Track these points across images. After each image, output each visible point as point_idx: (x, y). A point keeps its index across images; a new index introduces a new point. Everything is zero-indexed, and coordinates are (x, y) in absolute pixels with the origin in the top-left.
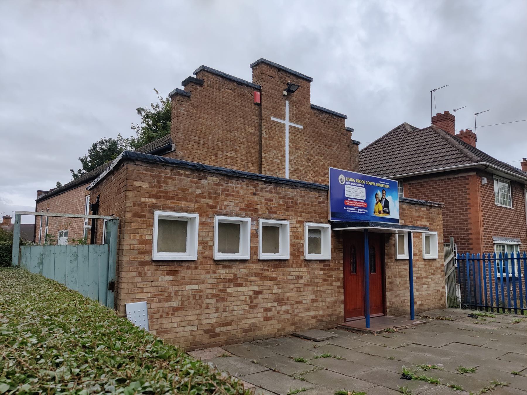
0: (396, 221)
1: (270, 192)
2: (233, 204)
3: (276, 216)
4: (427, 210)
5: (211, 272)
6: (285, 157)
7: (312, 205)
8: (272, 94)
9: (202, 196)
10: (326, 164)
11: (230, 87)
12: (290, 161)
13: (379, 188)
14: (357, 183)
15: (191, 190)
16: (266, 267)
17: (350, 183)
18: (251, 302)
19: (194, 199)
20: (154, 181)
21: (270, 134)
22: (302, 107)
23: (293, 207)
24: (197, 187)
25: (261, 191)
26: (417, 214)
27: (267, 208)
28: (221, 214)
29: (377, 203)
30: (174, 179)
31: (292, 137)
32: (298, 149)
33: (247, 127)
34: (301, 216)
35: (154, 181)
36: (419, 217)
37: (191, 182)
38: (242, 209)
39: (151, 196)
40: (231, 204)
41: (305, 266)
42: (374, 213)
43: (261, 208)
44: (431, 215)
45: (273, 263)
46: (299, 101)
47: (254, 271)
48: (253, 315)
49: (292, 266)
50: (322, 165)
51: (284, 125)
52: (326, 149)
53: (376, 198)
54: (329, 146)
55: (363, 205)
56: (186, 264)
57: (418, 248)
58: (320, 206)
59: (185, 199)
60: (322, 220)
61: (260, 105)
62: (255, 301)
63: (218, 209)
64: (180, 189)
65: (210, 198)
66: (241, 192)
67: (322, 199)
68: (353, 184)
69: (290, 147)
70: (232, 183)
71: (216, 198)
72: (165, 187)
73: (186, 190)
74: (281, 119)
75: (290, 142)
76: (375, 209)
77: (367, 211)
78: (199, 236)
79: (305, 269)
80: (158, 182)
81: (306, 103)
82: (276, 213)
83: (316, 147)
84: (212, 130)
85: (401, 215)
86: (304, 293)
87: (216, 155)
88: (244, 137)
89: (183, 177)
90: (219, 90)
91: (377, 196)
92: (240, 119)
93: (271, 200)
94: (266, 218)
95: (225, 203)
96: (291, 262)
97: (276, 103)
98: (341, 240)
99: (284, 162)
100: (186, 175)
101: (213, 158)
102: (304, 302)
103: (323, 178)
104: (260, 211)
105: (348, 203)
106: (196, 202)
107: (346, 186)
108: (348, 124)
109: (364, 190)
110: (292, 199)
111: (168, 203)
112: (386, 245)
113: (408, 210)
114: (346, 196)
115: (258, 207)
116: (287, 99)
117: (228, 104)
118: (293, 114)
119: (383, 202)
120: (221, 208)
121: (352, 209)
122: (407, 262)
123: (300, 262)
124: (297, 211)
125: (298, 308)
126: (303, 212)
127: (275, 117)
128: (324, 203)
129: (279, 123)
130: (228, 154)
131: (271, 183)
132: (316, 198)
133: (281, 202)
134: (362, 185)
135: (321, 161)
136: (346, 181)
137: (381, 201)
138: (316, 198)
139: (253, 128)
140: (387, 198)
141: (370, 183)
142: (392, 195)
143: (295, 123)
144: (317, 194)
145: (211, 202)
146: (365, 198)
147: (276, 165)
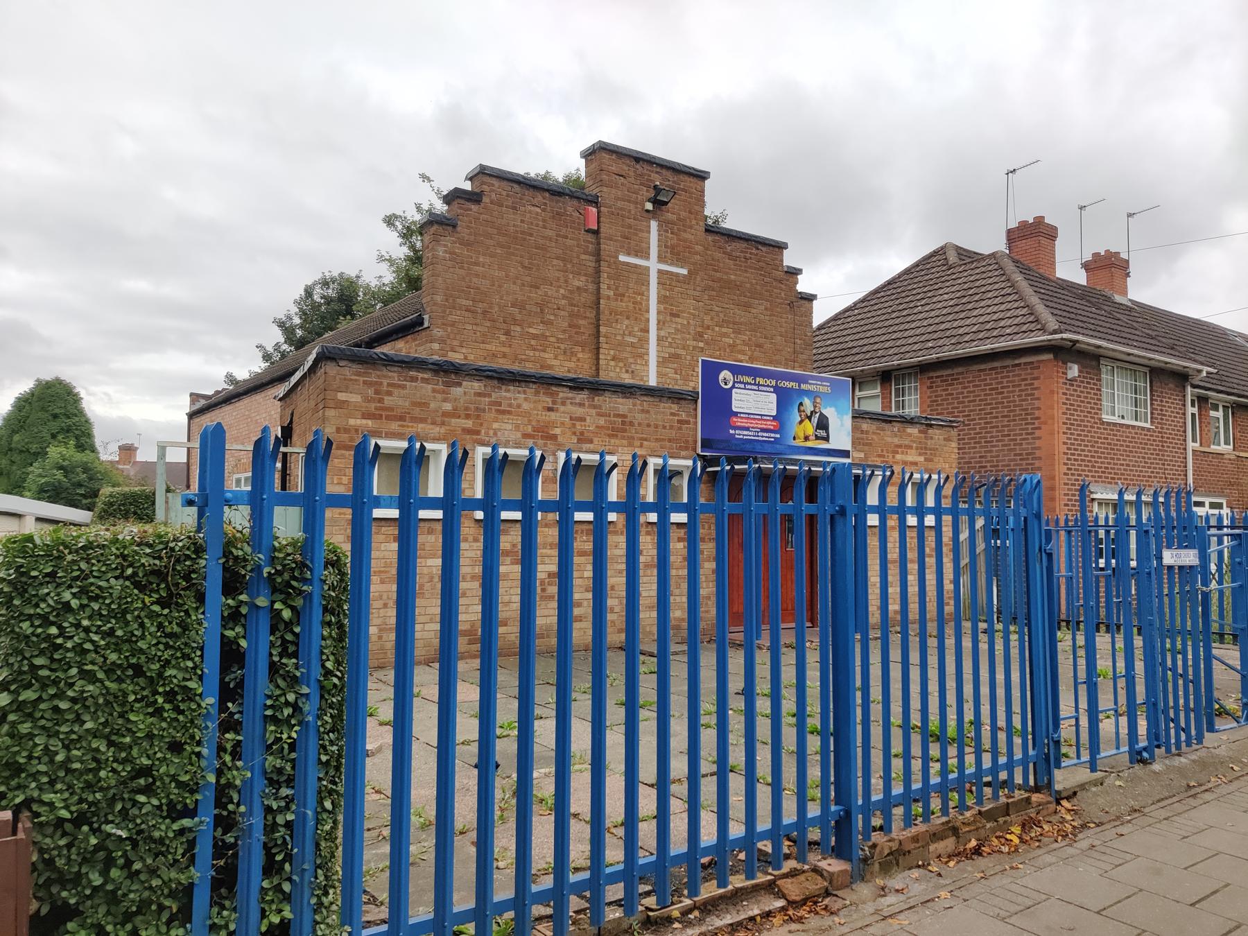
0: (845, 454)
1: (581, 405)
2: (509, 427)
3: (591, 446)
4: (920, 432)
5: (471, 538)
6: (648, 331)
7: (664, 427)
8: (621, 209)
9: (454, 414)
11: (535, 202)
12: (659, 339)
14: (759, 385)
15: (432, 405)
19: (439, 420)
20: (370, 392)
21: (617, 289)
23: (625, 431)
24: (445, 400)
25: (563, 404)
26: (896, 441)
27: (574, 433)
30: (404, 387)
31: (663, 292)
32: (678, 316)
34: (641, 446)
35: (370, 392)
36: (900, 446)
37: (434, 391)
39: (366, 416)
43: (563, 433)
44: (929, 442)
46: (679, 219)
50: (730, 346)
51: (648, 269)
54: (747, 306)
55: (771, 425)
56: (427, 525)
58: (680, 429)
59: (423, 420)
60: (683, 453)
61: (596, 233)
63: (483, 436)
64: (414, 404)
65: (468, 417)
66: (525, 406)
67: (684, 416)
69: (659, 313)
70: (509, 391)
71: (478, 417)
72: (388, 401)
73: (424, 405)
74: (641, 257)
75: (659, 302)
80: (377, 392)
81: (694, 222)
82: (591, 442)
84: (500, 286)
85: (854, 443)
87: (507, 333)
88: (564, 297)
89: (419, 384)
90: (514, 208)
92: (555, 262)
93: (582, 419)
95: (495, 425)
97: (630, 227)
99: (647, 341)
100: (425, 380)
101: (503, 338)
104: (560, 439)
105: (738, 422)
106: (443, 424)
109: (774, 397)
110: (624, 416)
115: (557, 431)
116: (654, 218)
117: (531, 235)
118: (666, 247)
119: (815, 419)
120: (487, 434)
124: (633, 438)
127: (629, 254)
128: (688, 422)
129: (636, 266)
130: (531, 330)
131: (582, 389)
132: (672, 414)
133: (602, 422)
137: (809, 418)
138: (672, 414)
139: (583, 278)
142: (836, 407)
143: (671, 264)
144: (675, 407)
145: (469, 424)
146: (774, 413)
147: (629, 349)
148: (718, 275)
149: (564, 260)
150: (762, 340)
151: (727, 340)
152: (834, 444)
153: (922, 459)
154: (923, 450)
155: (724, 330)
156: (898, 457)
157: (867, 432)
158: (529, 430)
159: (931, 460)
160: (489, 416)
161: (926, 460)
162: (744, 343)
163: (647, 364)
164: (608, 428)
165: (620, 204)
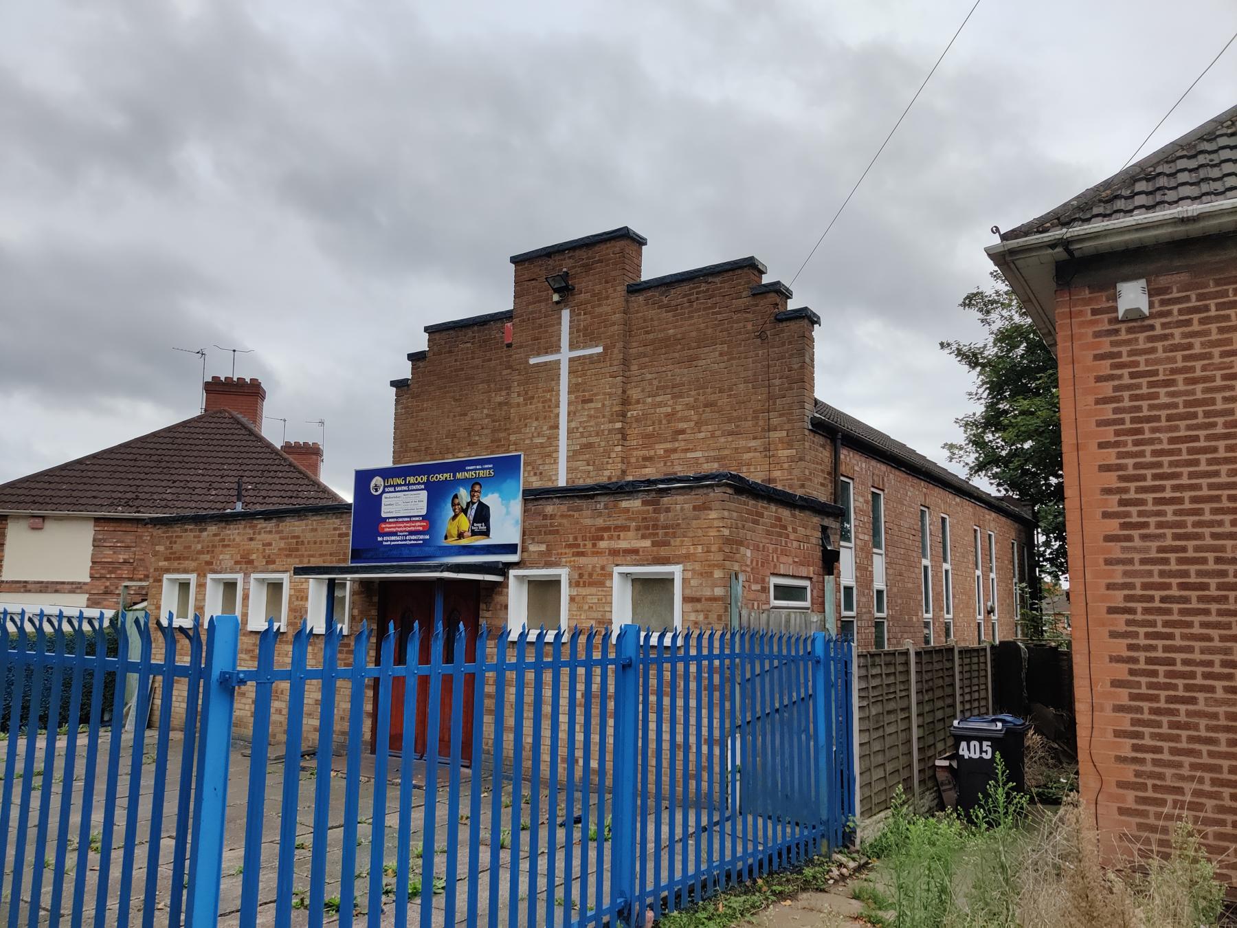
0: (511, 549)
1: (270, 532)
4: (644, 503)
6: (557, 427)
8: (532, 313)
10: (679, 408)
11: (466, 339)
12: (570, 431)
13: (462, 482)
14: (409, 484)
17: (392, 489)
22: (600, 305)
23: (297, 550)
26: (600, 522)
28: (215, 572)
31: (574, 381)
32: (591, 401)
36: (607, 529)
39: (167, 559)
40: (226, 558)
42: (446, 538)
44: (662, 517)
46: (594, 295)
50: (668, 415)
51: (571, 360)
53: (453, 505)
55: (419, 526)
58: (340, 542)
59: (186, 559)
63: (214, 566)
64: (185, 547)
69: (569, 404)
74: (552, 353)
75: (569, 393)
82: (274, 562)
83: (649, 376)
90: (450, 352)
91: (457, 501)
92: (480, 386)
93: (270, 544)
98: (376, 599)
99: (556, 438)
103: (669, 446)
105: (386, 528)
108: (405, 371)
110: (298, 537)
111: (175, 564)
112: (483, 606)
113: (562, 516)
114: (383, 515)
115: (254, 556)
116: (566, 307)
117: (462, 369)
119: (472, 512)
121: (393, 538)
124: (303, 556)
126: (312, 556)
127: (538, 355)
129: (546, 363)
132: (335, 529)
133: (282, 545)
135: (666, 405)
137: (465, 511)
138: (335, 529)
140: (484, 500)
142: (500, 492)
143: (583, 348)
144: (338, 521)
146: (424, 512)
147: (537, 451)
148: (651, 336)
149: (488, 382)
150: (713, 397)
151: (663, 410)
152: (495, 538)
153: (647, 543)
154: (647, 528)
155: (658, 399)
156: (603, 544)
157: (552, 517)
159: (666, 544)
160: (217, 550)
161: (654, 544)
162: (689, 407)
163: (556, 462)
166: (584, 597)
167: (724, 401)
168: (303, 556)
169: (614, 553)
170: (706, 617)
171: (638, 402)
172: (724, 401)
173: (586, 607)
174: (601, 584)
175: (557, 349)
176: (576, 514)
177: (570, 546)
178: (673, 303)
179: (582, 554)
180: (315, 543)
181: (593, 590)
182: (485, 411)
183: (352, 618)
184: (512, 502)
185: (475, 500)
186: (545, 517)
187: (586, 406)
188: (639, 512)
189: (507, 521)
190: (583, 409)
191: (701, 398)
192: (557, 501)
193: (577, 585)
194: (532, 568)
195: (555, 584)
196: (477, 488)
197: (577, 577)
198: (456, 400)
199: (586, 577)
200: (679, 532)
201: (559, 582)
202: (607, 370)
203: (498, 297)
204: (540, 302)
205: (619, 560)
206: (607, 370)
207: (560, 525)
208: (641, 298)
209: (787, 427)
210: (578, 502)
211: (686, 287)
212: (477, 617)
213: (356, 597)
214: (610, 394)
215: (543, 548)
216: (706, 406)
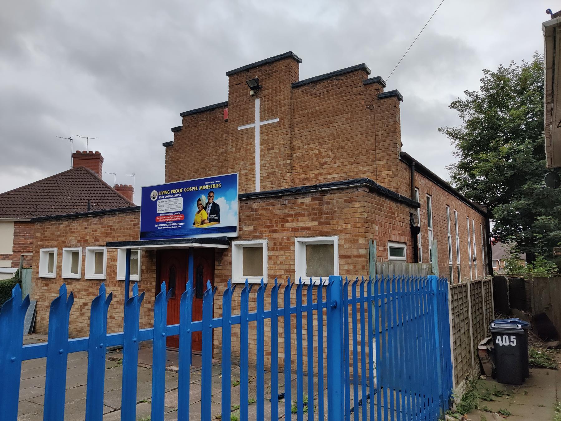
0: (232, 229)
1: (96, 224)
2: (74, 238)
4: (313, 199)
6: (254, 164)
8: (239, 102)
10: (323, 150)
11: (203, 119)
12: (261, 166)
13: (203, 191)
14: (173, 194)
16: (91, 285)
17: (163, 197)
18: (81, 310)
21: (237, 146)
22: (277, 96)
23: (111, 233)
26: (286, 212)
27: (93, 238)
28: (67, 247)
29: (199, 212)
31: (263, 138)
32: (273, 149)
33: (218, 148)
36: (291, 216)
38: (79, 241)
39: (42, 240)
40: (73, 239)
41: (119, 286)
42: (194, 224)
43: (90, 238)
44: (324, 207)
45: (96, 282)
47: (84, 288)
48: (82, 321)
49: (109, 285)
50: (316, 155)
51: (261, 127)
52: (322, 130)
53: (198, 205)
55: (179, 218)
57: (286, 267)
58: (134, 228)
59: (52, 240)
62: (84, 311)
63: (67, 244)
64: (51, 234)
68: (167, 197)
69: (261, 151)
74: (250, 123)
75: (261, 145)
76: (196, 220)
77: (184, 224)
78: (58, 262)
79: (119, 288)
83: (306, 134)
86: (117, 310)
90: (194, 126)
91: (200, 203)
92: (211, 144)
94: (92, 246)
95: (70, 238)
96: (108, 282)
97: (244, 109)
98: (155, 260)
99: (254, 170)
102: (116, 318)
103: (317, 172)
105: (159, 219)
107: (158, 201)
109: (181, 200)
110: (111, 226)
111: (46, 243)
112: (216, 263)
113: (263, 209)
114: (158, 212)
115: (88, 238)
117: (201, 135)
119: (209, 209)
121: (164, 225)
122: (124, 285)
123: (115, 282)
124: (114, 237)
125: (111, 322)
126: (119, 236)
127: (243, 125)
132: (131, 221)
133: (103, 231)
134: (177, 195)
135: (315, 149)
136: (159, 196)
137: (205, 208)
138: (131, 221)
140: (216, 201)
141: (190, 189)
142: (225, 196)
143: (268, 120)
144: (133, 217)
146: (181, 210)
148: (306, 111)
149: (215, 141)
150: (343, 143)
151: (314, 152)
152: (223, 223)
153: (316, 223)
154: (315, 214)
155: (311, 146)
156: (288, 225)
157: (257, 210)
158: (79, 239)
159: (327, 223)
161: (320, 224)
162: (329, 149)
163: (254, 183)
164: (105, 233)
165: (238, 100)
166: (277, 257)
167: (349, 145)
168: (114, 237)
169: (295, 230)
170: (355, 267)
171: (299, 148)
172: (349, 145)
173: (279, 262)
174: (287, 249)
175: (253, 121)
176: (271, 208)
177: (268, 227)
178: (318, 92)
179: (275, 231)
180: (121, 229)
181: (283, 252)
182: (214, 157)
183: (142, 271)
184: (233, 202)
185: (211, 201)
186: (252, 210)
187: (270, 152)
188: (310, 205)
189: (230, 213)
190: (269, 153)
191: (336, 144)
192: (259, 200)
193: (273, 249)
194: (245, 240)
195: (259, 249)
196: (212, 194)
197: (272, 245)
198: (198, 152)
199: (278, 244)
200: (335, 216)
201: (262, 248)
202: (281, 131)
203: (221, 94)
204: (243, 96)
205: (298, 234)
206: (281, 131)
207: (261, 214)
208: (300, 91)
209: (386, 158)
210: (272, 201)
211: (325, 83)
212: (213, 269)
213: (144, 259)
214: (283, 144)
215: (252, 228)
216: (338, 148)
